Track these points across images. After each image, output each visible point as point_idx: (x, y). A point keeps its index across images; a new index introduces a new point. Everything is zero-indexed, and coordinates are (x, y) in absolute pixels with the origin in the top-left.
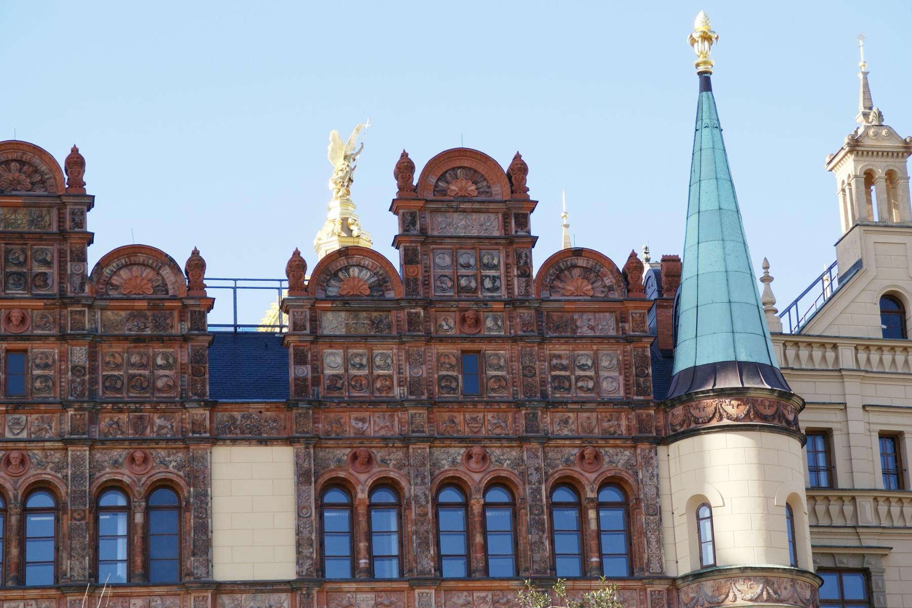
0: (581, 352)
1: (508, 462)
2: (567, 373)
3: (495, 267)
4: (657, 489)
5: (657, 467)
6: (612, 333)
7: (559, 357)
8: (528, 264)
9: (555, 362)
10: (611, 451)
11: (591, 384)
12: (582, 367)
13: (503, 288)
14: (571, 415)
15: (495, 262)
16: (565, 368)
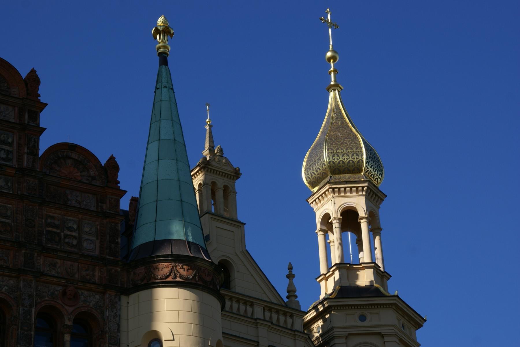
0: (69, 218)
1: (6, 287)
2: (58, 231)
3: (10, 144)
4: (119, 326)
5: (120, 310)
6: (93, 209)
7: (53, 218)
8: (36, 146)
9: (49, 221)
10: (86, 293)
11: (75, 242)
12: (70, 229)
13: (15, 160)
14: (58, 261)
15: (10, 140)
16: (56, 227)
